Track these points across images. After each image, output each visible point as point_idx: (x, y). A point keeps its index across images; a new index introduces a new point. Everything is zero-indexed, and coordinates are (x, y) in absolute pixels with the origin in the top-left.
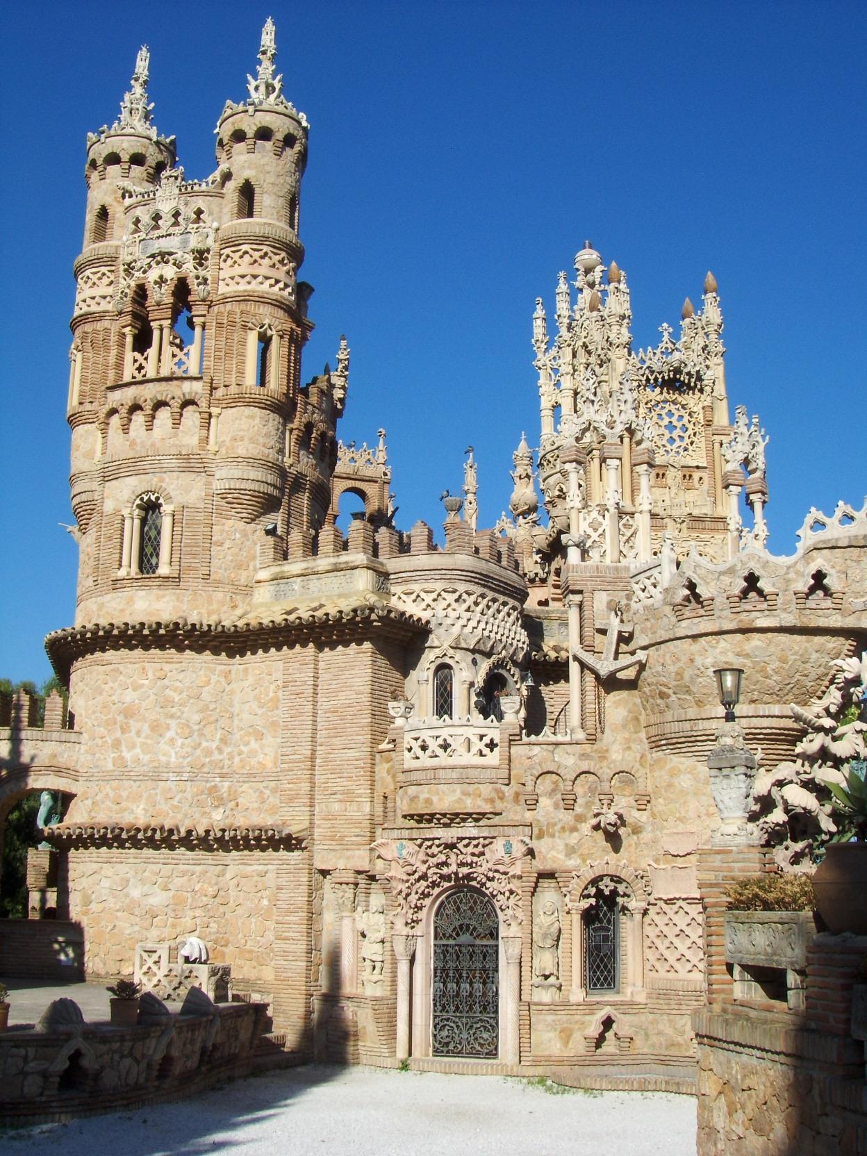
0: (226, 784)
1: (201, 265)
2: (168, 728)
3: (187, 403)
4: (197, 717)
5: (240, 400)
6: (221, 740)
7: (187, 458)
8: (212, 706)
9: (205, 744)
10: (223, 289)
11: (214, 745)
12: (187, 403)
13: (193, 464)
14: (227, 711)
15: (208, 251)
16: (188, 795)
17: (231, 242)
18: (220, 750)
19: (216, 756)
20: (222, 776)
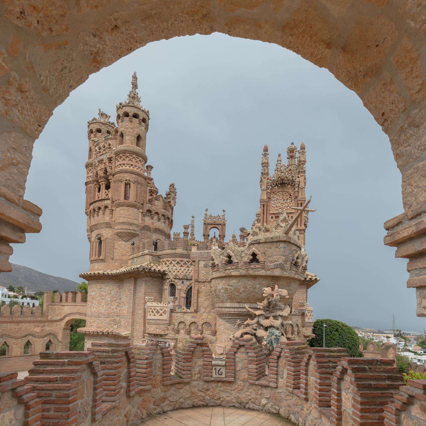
0: (118, 318)
1: (110, 163)
2: (102, 303)
3: (106, 207)
4: (109, 299)
5: (120, 205)
6: (117, 306)
7: (107, 224)
8: (114, 296)
9: (112, 307)
10: (117, 170)
11: (115, 307)
12: (106, 207)
13: (108, 225)
14: (118, 297)
15: (112, 157)
16: (107, 321)
17: (117, 154)
18: (116, 309)
19: (115, 310)
20: (117, 316)
